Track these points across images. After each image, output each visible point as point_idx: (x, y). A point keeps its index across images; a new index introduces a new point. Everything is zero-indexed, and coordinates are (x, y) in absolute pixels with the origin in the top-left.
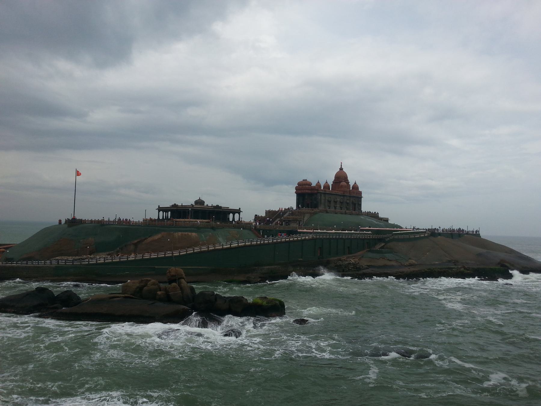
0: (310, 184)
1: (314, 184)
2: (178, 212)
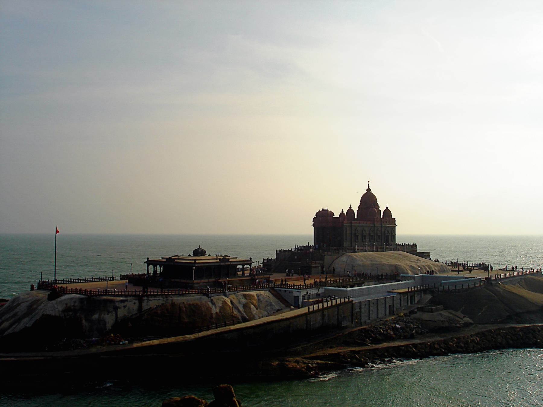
1: (337, 215)
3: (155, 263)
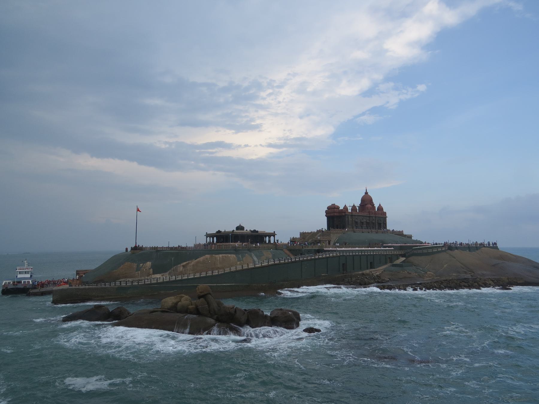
0: (338, 208)
1: (341, 208)
2: (222, 237)
3: (211, 236)
